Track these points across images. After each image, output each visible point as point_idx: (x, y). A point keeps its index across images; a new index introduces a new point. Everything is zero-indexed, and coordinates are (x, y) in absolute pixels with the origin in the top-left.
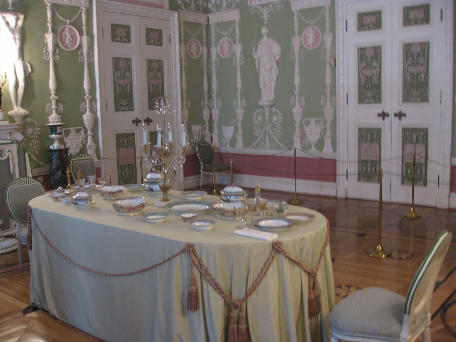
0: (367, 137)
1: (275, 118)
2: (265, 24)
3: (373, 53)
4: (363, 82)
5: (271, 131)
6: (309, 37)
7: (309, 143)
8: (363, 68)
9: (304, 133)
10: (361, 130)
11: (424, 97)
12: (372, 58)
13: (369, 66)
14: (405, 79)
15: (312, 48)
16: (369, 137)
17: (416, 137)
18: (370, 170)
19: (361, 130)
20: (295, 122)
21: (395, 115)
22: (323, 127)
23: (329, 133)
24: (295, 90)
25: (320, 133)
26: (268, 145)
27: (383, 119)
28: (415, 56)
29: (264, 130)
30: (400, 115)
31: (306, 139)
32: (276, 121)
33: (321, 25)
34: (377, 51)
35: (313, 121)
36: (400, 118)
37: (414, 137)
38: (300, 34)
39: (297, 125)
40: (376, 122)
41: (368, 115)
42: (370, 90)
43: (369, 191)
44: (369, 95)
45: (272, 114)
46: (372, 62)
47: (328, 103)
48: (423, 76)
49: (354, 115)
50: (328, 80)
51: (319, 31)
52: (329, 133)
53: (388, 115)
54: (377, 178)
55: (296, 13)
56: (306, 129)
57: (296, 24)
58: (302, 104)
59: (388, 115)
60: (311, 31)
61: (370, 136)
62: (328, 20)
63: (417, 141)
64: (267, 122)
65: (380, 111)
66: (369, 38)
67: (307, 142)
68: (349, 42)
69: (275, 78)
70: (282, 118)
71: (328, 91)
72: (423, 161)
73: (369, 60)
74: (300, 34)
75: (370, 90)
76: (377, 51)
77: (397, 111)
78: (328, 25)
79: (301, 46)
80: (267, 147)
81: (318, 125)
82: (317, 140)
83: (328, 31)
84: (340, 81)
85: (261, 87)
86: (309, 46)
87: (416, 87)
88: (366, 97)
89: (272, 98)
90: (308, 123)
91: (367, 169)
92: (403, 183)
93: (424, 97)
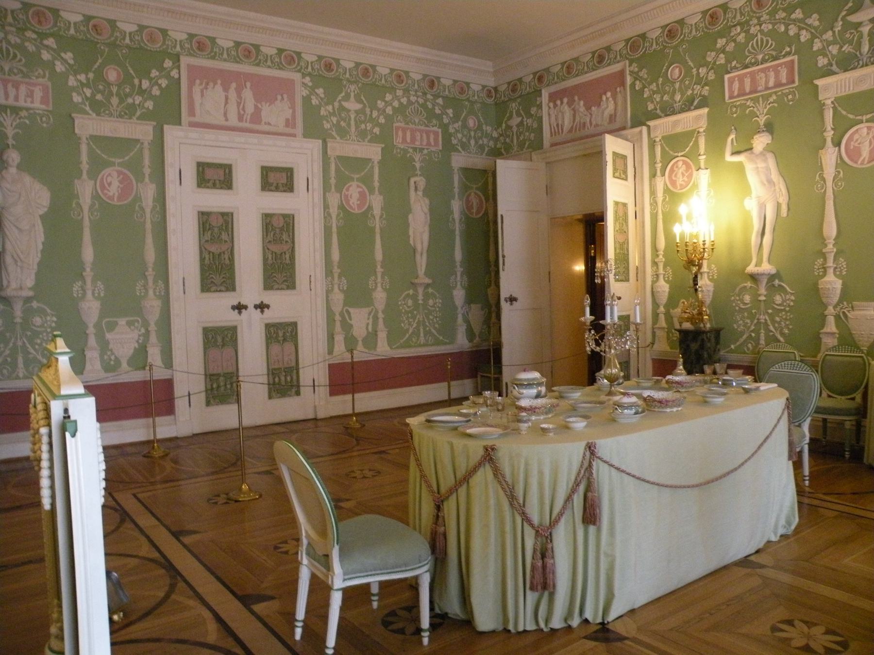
0: (216, 341)
1: (38, 320)
2: (10, 143)
3: (221, 220)
4: (207, 262)
5: (28, 346)
6: (110, 184)
7: (118, 361)
8: (207, 241)
9: (107, 343)
10: (206, 331)
11: (290, 284)
12: (220, 229)
13: (214, 240)
14: (265, 259)
15: (115, 202)
16: (219, 339)
17: (282, 334)
18: (222, 387)
19: (206, 331)
20: (87, 327)
21: (256, 307)
22: (143, 331)
23: (153, 338)
24: (84, 270)
25: (137, 342)
26: (21, 372)
27: (240, 313)
28: (278, 230)
29: (11, 344)
30: (262, 307)
31: (109, 353)
32: (42, 326)
33: (135, 166)
34: (227, 220)
35: (122, 322)
36: (262, 312)
37: (281, 334)
38: (93, 174)
39: (91, 330)
40: (230, 318)
41: (217, 309)
42: (217, 272)
43: (224, 417)
44: (218, 279)
45: (28, 313)
46: (221, 234)
47: (151, 292)
48: (287, 256)
49: (195, 310)
50: (150, 254)
51: (132, 177)
52: (153, 338)
53: (246, 307)
54: (235, 397)
55: (84, 139)
56: (108, 336)
57: (84, 158)
58: (99, 294)
59: (246, 307)
60: (115, 174)
61: (221, 339)
62: (147, 162)
63: (285, 340)
64: (18, 327)
65: (235, 303)
66: (215, 200)
67: (113, 358)
68: (186, 203)
69: (41, 247)
70: (55, 319)
71: (150, 273)
72: (293, 364)
73: (216, 230)
74: (93, 174)
75: (217, 272)
76: (227, 220)
77: (258, 303)
78: (147, 171)
79: (96, 196)
80: (21, 375)
81: (132, 327)
82: (132, 351)
83: (147, 180)
84: (173, 257)
85: (8, 259)
86: (110, 198)
87: (279, 271)
88: (212, 282)
89: (30, 282)
90: (112, 327)
91: (219, 387)
92: (270, 397)
93: (290, 284)
